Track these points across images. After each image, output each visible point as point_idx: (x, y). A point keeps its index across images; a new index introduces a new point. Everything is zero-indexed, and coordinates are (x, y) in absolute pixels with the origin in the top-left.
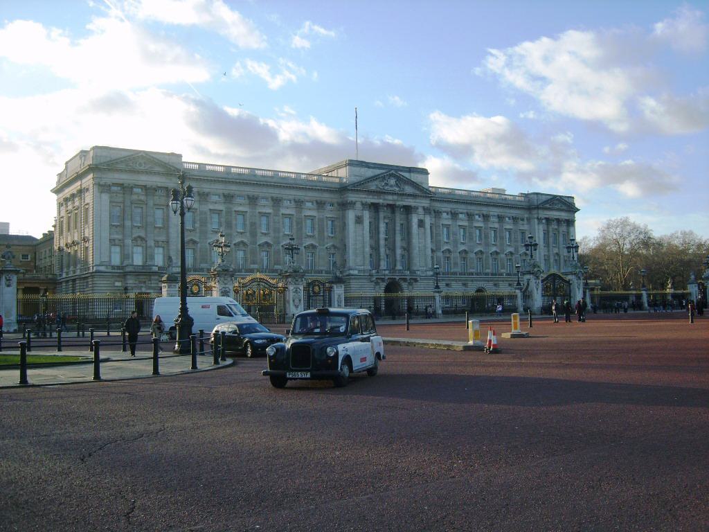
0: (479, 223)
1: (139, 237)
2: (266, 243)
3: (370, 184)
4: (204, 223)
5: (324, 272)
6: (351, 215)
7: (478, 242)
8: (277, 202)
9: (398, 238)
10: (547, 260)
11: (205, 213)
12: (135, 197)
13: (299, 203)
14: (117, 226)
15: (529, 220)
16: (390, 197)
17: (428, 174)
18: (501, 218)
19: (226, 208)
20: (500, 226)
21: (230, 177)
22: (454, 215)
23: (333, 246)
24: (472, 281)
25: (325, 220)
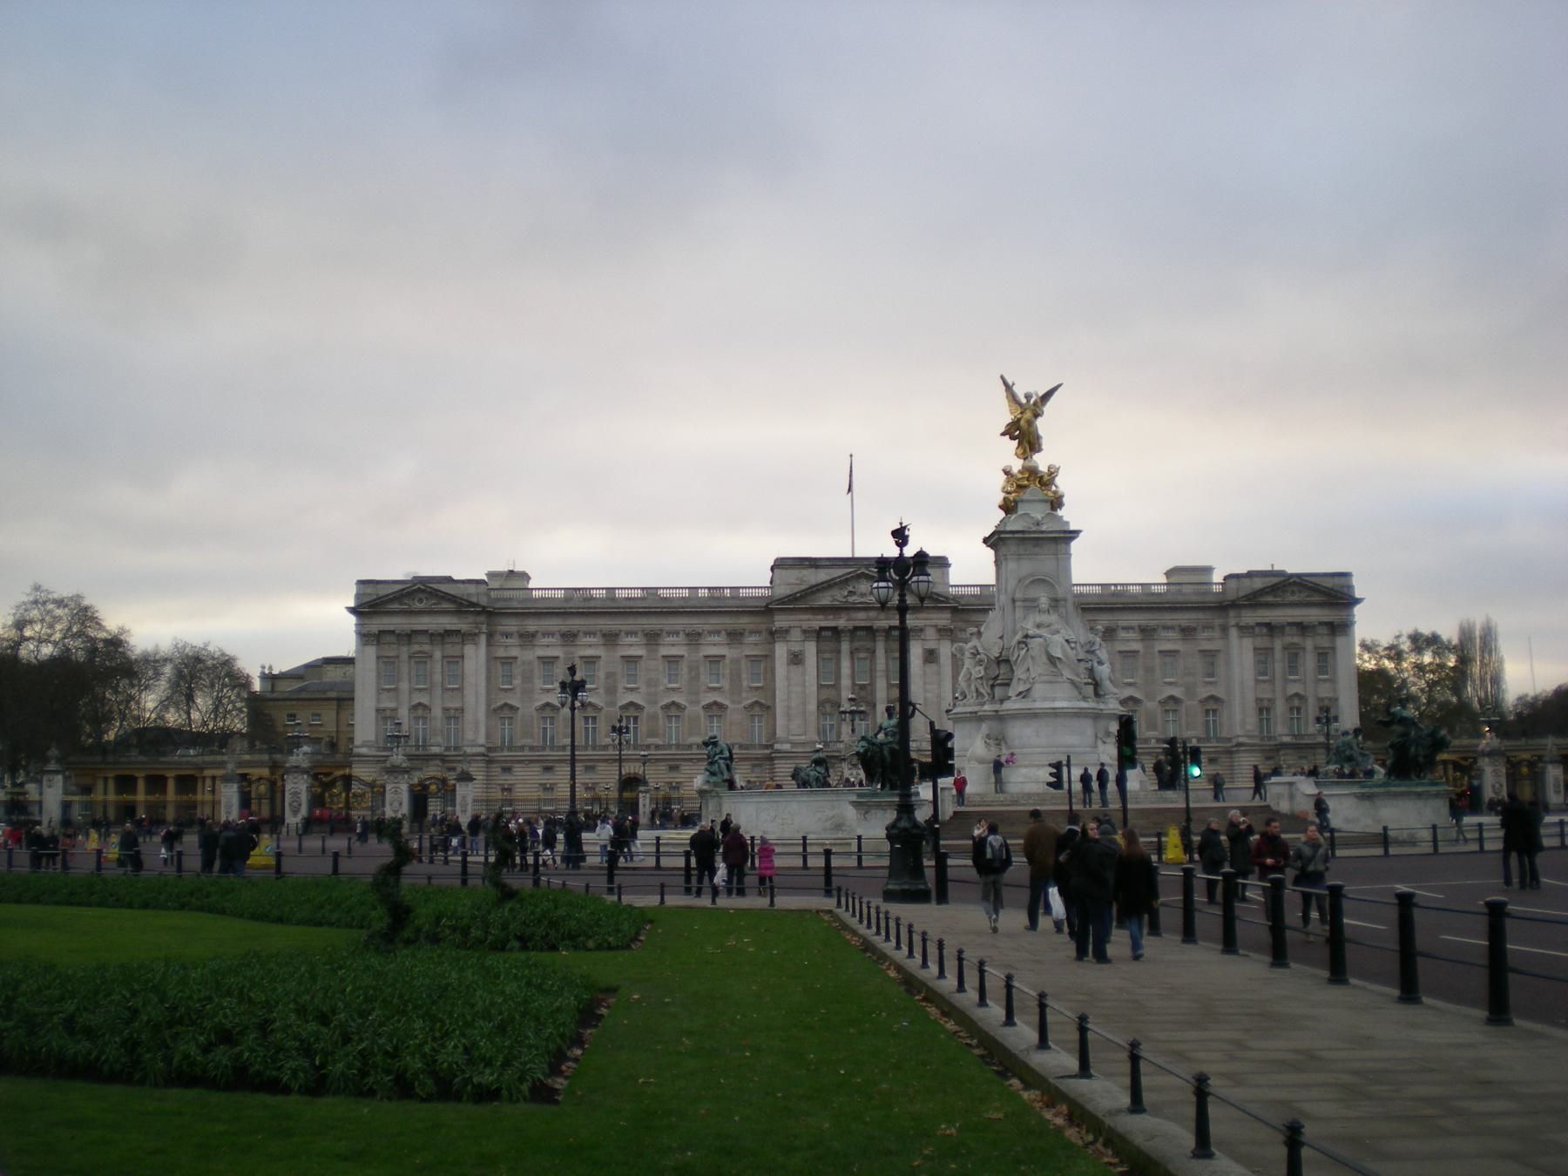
1: (420, 704)
2: (632, 704)
4: (527, 678)
6: (781, 651)
8: (653, 638)
10: (1264, 709)
11: (530, 663)
12: (416, 648)
13: (694, 638)
14: (389, 690)
16: (862, 615)
18: (1147, 633)
23: (756, 702)
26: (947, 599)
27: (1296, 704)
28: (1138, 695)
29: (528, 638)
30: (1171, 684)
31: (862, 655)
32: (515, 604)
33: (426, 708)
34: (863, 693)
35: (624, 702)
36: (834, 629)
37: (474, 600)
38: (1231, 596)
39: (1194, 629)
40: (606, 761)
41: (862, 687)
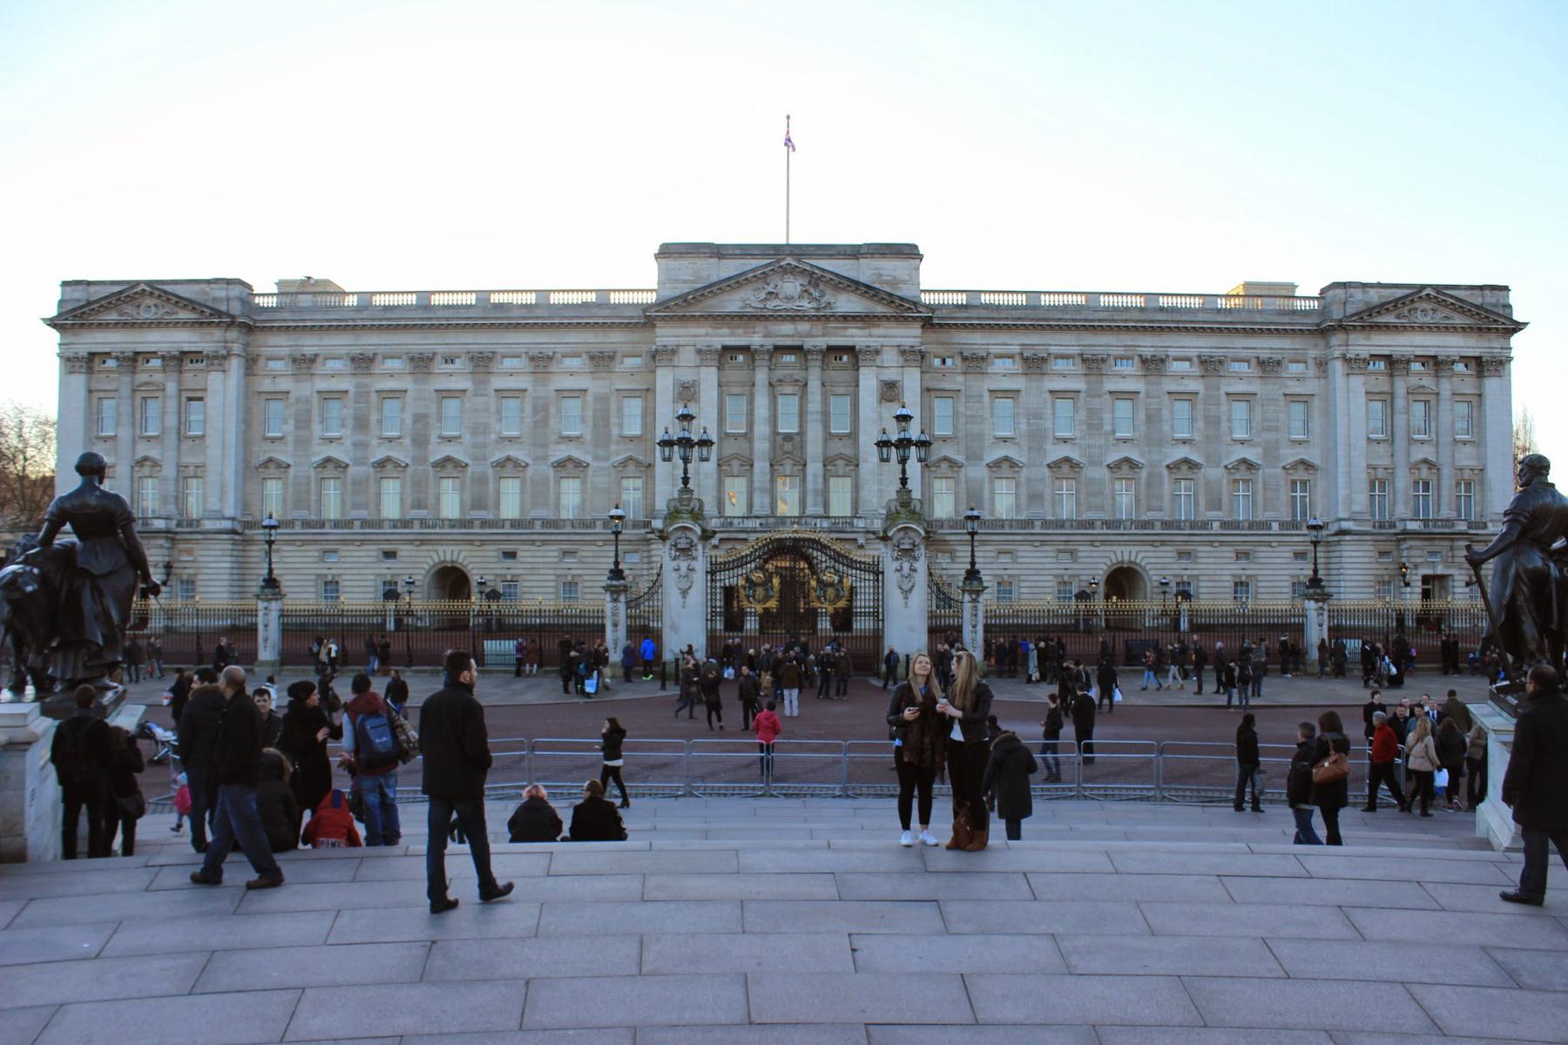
0: (1128, 377)
2: (448, 459)
3: (725, 297)
4: (303, 422)
5: (599, 523)
7: (1118, 435)
9: (814, 433)
10: (1379, 483)
11: (308, 401)
13: (541, 362)
15: (1322, 364)
16: (787, 328)
17: (920, 257)
19: (357, 386)
20: (1207, 388)
21: (364, 315)
22: (1034, 364)
23: (630, 458)
24: (1092, 543)
25: (613, 399)
26: (917, 304)
27: (1426, 476)
28: (1195, 457)
29: (304, 364)
30: (1242, 442)
31: (788, 389)
32: (287, 316)
33: (155, 464)
34: (788, 446)
35: (438, 457)
36: (745, 349)
37: (223, 308)
38: (1337, 313)
39: (1279, 363)
40: (411, 542)
41: (788, 437)
